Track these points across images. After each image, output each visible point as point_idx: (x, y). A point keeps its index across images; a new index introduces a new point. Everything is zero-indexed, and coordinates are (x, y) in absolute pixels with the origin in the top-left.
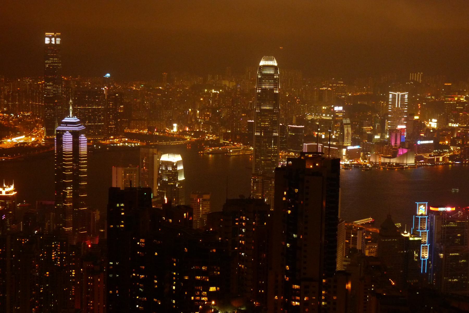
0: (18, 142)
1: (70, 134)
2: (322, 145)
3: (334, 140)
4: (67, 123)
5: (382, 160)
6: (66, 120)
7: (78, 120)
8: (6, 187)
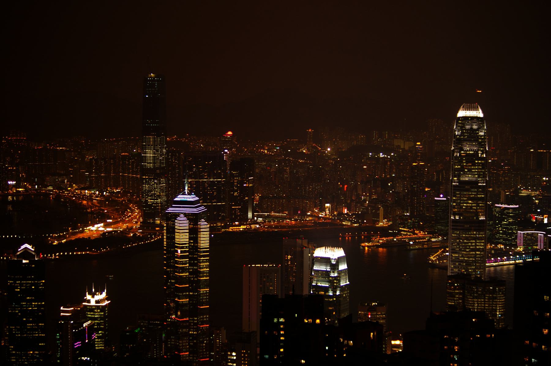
0: (106, 231)
2: (545, 233)
6: (180, 198)
7: (197, 198)
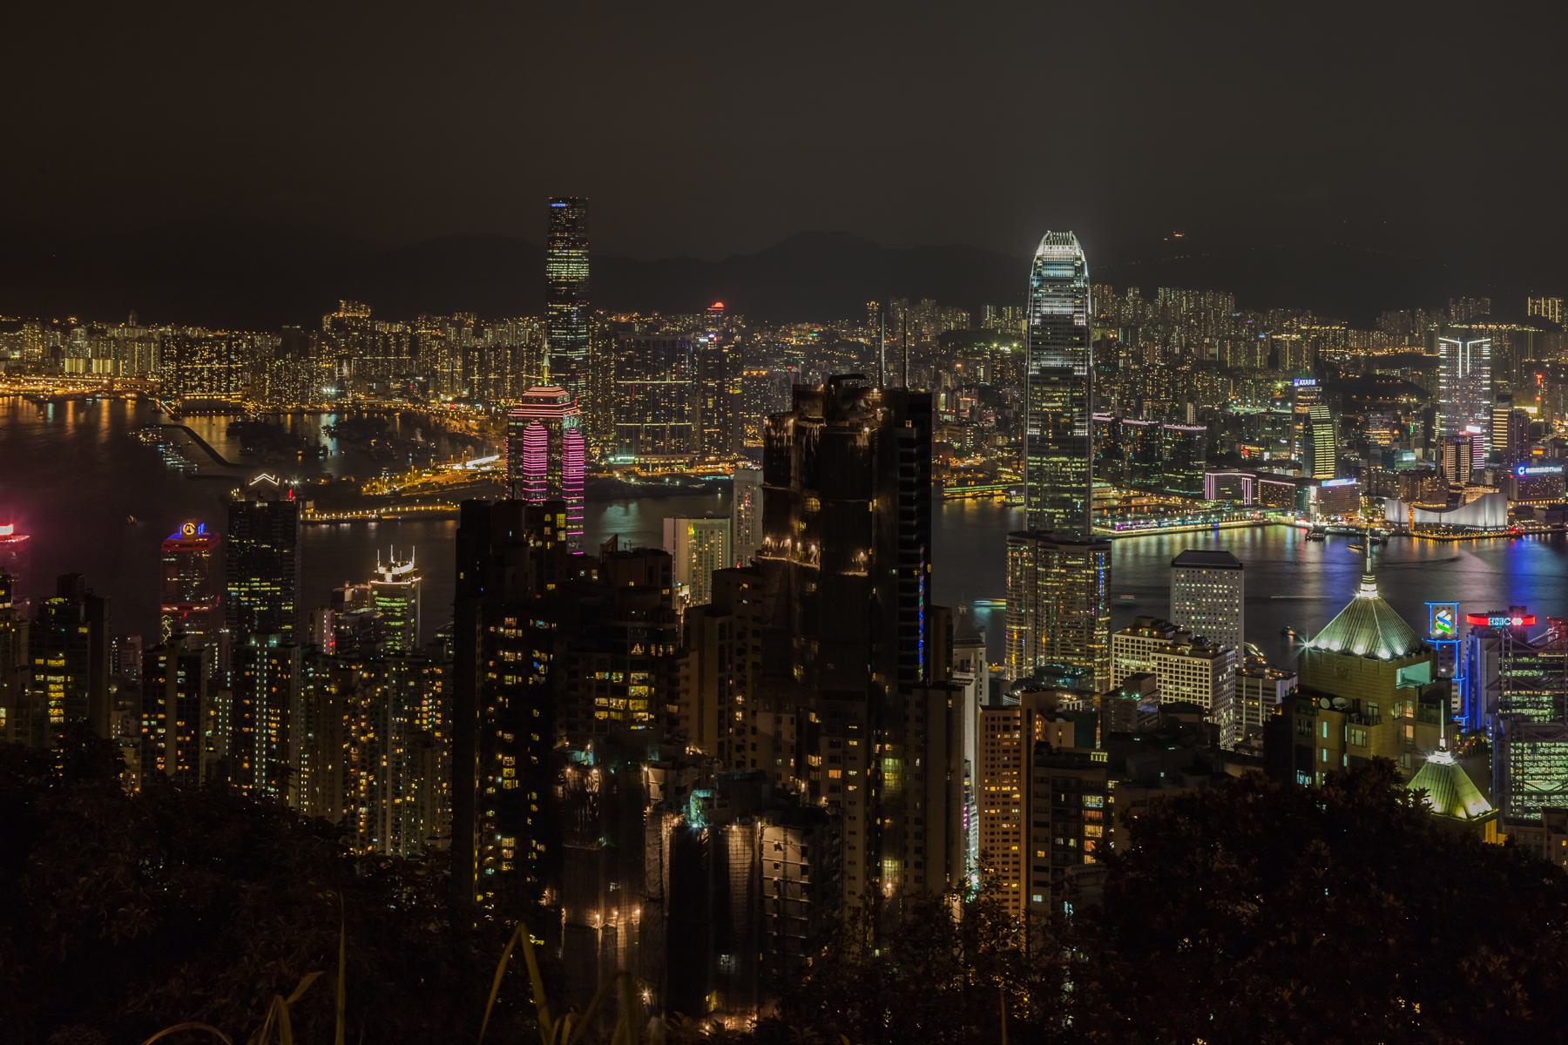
1: (541, 427)
3: (1294, 465)
4: (538, 399)
5: (1418, 517)
8: (395, 565)
